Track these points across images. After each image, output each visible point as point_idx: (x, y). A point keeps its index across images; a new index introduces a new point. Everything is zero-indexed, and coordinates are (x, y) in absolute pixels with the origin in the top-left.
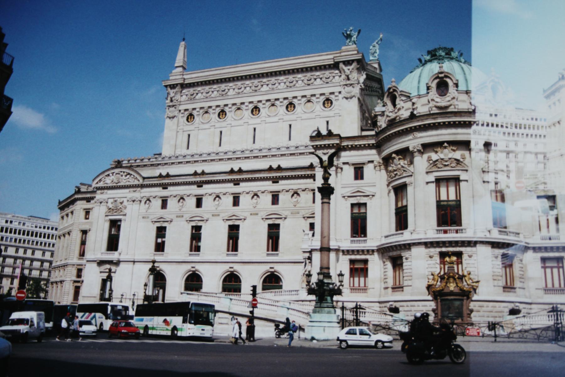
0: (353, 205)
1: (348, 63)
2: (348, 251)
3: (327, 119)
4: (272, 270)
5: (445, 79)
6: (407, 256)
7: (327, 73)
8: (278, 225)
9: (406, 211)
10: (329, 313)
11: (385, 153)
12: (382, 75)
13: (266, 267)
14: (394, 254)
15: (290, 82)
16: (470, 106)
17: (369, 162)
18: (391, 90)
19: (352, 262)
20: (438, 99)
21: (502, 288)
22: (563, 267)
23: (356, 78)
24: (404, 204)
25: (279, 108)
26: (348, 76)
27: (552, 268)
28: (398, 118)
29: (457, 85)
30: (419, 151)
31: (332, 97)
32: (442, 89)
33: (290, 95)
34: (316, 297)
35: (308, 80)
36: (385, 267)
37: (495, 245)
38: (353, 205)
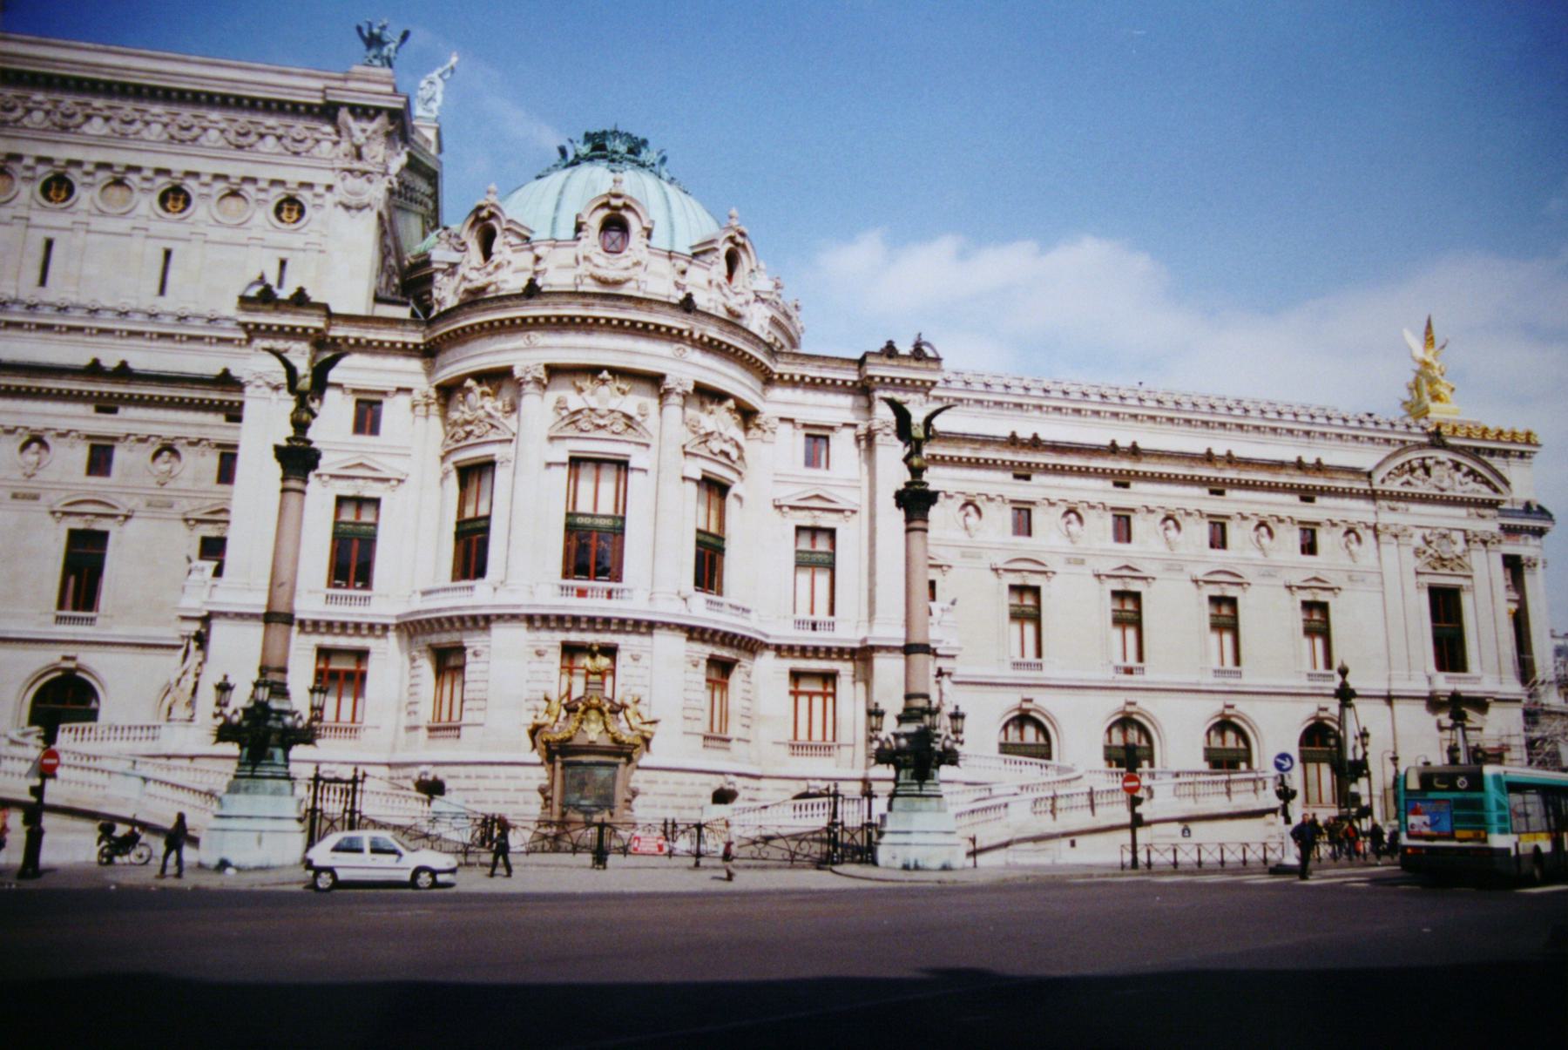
0: (341, 501)
1: (363, 112)
2: (316, 624)
3: (284, 254)
4: (71, 665)
5: (623, 213)
6: (479, 647)
7: (300, 127)
8: (104, 535)
9: (486, 530)
10: (277, 792)
11: (446, 373)
12: (440, 163)
13: (53, 656)
14: (445, 639)
15: (183, 128)
17: (399, 390)
18: (484, 214)
19: (324, 653)
20: (601, 259)
21: (701, 739)
22: (834, 695)
23: (380, 159)
24: (483, 511)
25: (137, 195)
26: (358, 149)
27: (811, 695)
28: (492, 288)
29: (649, 233)
30: (538, 381)
31: (305, 196)
32: (615, 235)
33: (178, 164)
34: (241, 748)
35: (239, 134)
36: (414, 672)
37: (695, 633)
38: (341, 501)
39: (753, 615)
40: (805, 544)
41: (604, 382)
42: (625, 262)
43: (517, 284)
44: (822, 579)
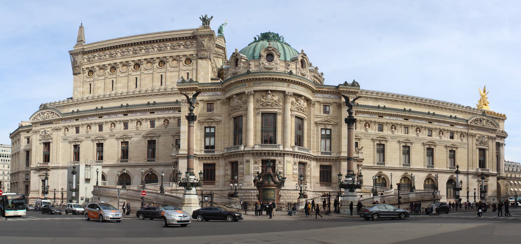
0: (205, 128)
11: (228, 95)
14: (233, 160)
32: (270, 57)
38: (205, 128)
39: (311, 151)
40: (323, 133)
41: (270, 94)
42: (274, 64)
43: (245, 71)
44: (328, 142)
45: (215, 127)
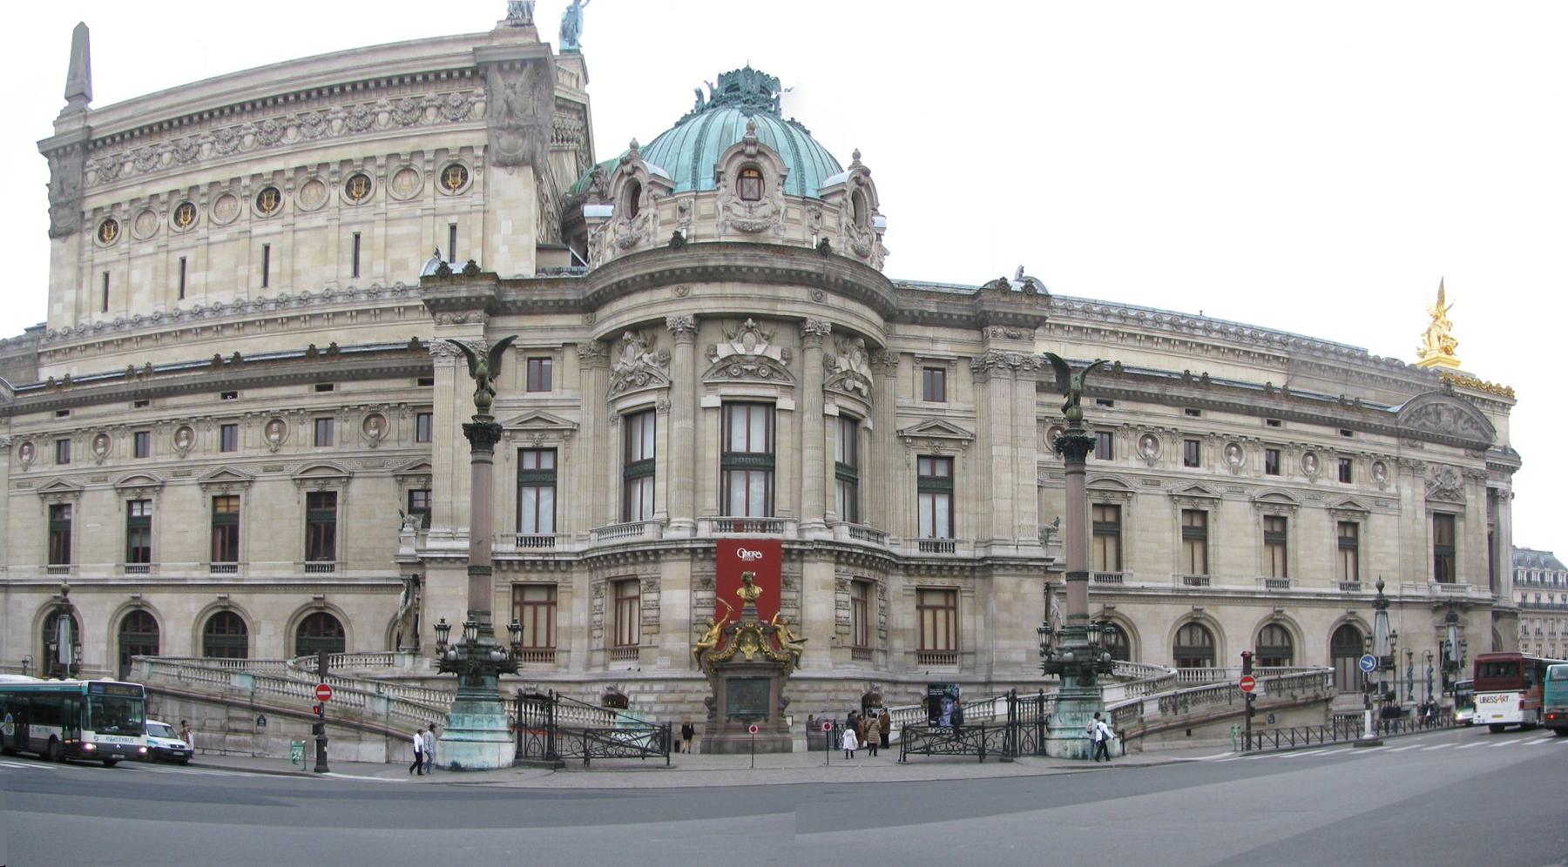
0: (521, 451)
14: (621, 572)
16: (808, 237)
24: (648, 455)
38: (521, 451)
41: (750, 329)
45: (554, 450)
